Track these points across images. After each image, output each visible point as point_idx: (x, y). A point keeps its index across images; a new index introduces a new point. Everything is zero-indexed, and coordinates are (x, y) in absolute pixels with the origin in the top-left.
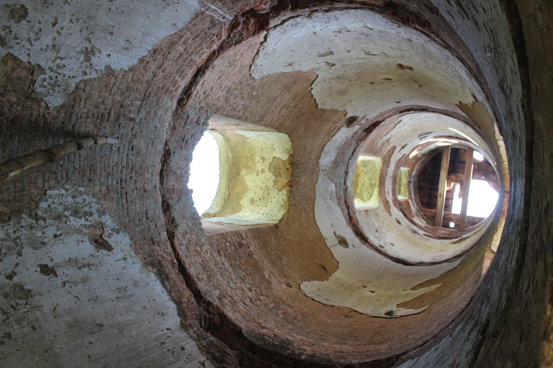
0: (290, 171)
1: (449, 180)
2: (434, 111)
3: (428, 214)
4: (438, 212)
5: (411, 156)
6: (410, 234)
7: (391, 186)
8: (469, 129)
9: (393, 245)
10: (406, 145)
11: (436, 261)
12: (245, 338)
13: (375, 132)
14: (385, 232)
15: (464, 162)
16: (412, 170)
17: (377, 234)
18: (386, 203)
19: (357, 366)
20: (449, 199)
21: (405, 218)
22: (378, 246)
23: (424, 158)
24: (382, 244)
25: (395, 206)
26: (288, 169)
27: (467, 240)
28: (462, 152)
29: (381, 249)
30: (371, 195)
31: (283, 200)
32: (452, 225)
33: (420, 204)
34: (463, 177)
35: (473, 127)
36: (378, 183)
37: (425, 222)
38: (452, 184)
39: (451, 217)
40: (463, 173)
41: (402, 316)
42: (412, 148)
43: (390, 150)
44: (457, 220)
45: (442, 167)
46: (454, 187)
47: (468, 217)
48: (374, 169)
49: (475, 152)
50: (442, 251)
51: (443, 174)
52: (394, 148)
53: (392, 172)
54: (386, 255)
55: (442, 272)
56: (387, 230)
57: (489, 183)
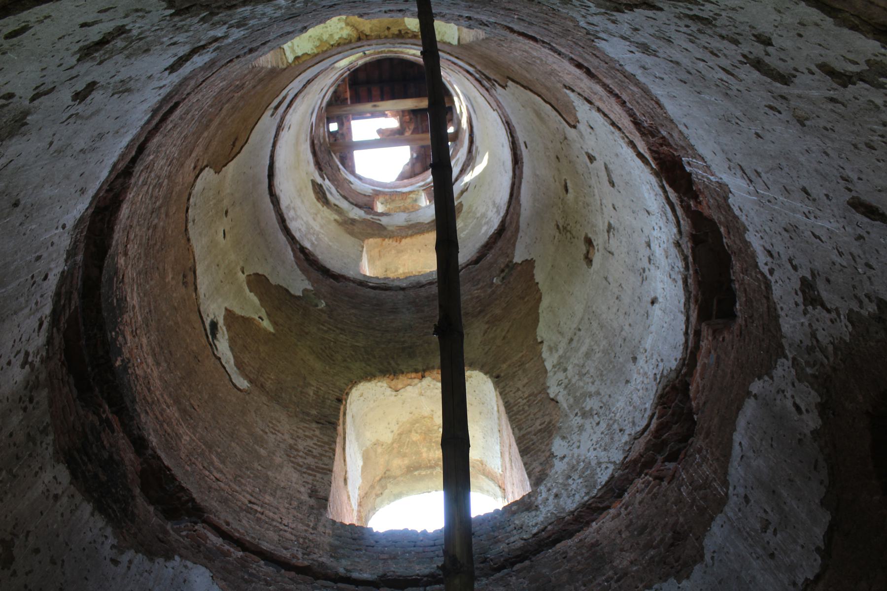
0: (386, 33)
1: (402, 114)
12: (101, 268)
19: (150, 452)
26: (388, 29)
31: (331, 35)
32: (334, 127)
39: (345, 124)
41: (219, 359)
44: (342, 134)
47: (352, 156)
51: (409, 104)
57: (407, 164)
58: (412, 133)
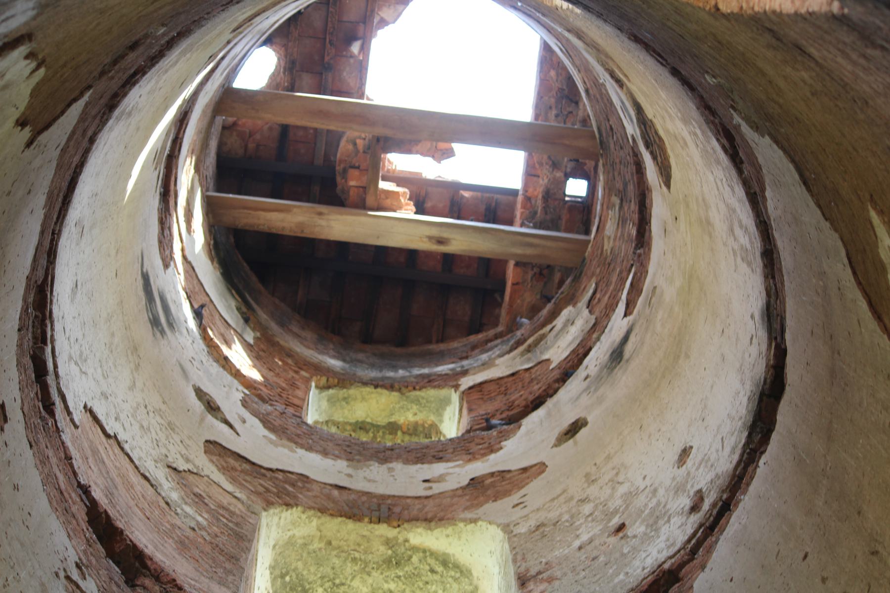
2: (48, 253)
3: (529, 298)
4: (519, 251)
5: (254, 374)
6: (626, 378)
7: (398, 466)
8: (139, 96)
9: (685, 453)
10: (200, 393)
11: (758, 244)
13: (142, 536)
14: (622, 490)
15: (285, 129)
16: (318, 369)
17: (637, 529)
18: (480, 490)
20: (453, 201)
21: (550, 403)
22: (695, 519)
23: (263, 316)
24: (686, 502)
25: (492, 449)
27: (649, 113)
28: (234, 142)
29: (706, 506)
30: (445, 561)
32: (577, 188)
33: (481, 336)
34: (354, 137)
35: (131, 81)
36: (383, 530)
37: (566, 313)
38: (383, 185)
39: (538, 192)
40: (334, 138)
42: (215, 369)
43: (224, 469)
44: (555, 165)
45: (307, 234)
46: (400, 180)
48: (316, 545)
49: (240, 83)
50: (706, 224)
51: (339, 226)
52: (213, 447)
53: (328, 462)
54: (738, 481)
55: (811, 215)
56: (615, 483)
57: (383, 23)
58: (344, 133)
